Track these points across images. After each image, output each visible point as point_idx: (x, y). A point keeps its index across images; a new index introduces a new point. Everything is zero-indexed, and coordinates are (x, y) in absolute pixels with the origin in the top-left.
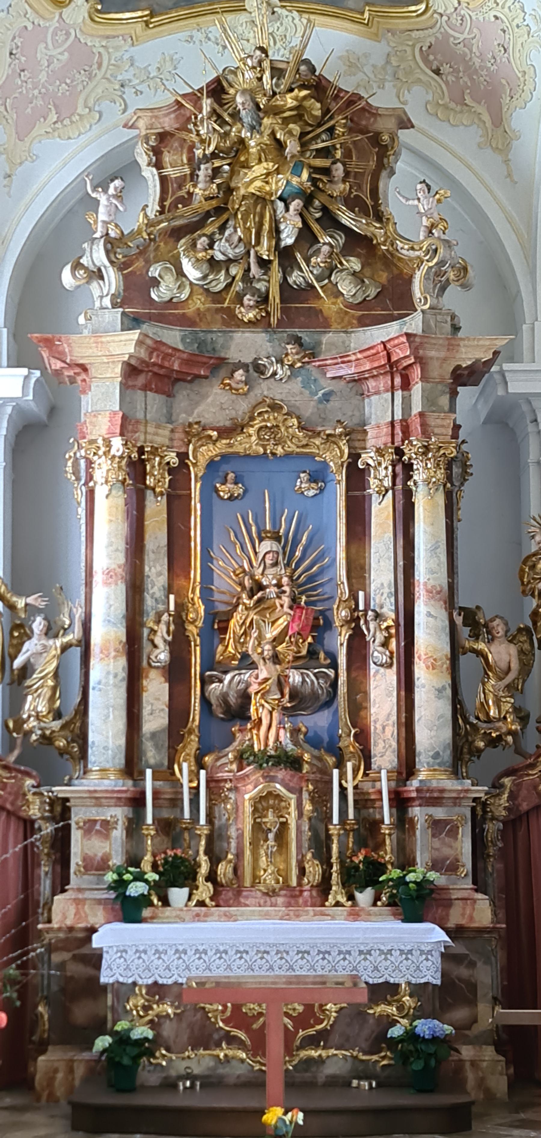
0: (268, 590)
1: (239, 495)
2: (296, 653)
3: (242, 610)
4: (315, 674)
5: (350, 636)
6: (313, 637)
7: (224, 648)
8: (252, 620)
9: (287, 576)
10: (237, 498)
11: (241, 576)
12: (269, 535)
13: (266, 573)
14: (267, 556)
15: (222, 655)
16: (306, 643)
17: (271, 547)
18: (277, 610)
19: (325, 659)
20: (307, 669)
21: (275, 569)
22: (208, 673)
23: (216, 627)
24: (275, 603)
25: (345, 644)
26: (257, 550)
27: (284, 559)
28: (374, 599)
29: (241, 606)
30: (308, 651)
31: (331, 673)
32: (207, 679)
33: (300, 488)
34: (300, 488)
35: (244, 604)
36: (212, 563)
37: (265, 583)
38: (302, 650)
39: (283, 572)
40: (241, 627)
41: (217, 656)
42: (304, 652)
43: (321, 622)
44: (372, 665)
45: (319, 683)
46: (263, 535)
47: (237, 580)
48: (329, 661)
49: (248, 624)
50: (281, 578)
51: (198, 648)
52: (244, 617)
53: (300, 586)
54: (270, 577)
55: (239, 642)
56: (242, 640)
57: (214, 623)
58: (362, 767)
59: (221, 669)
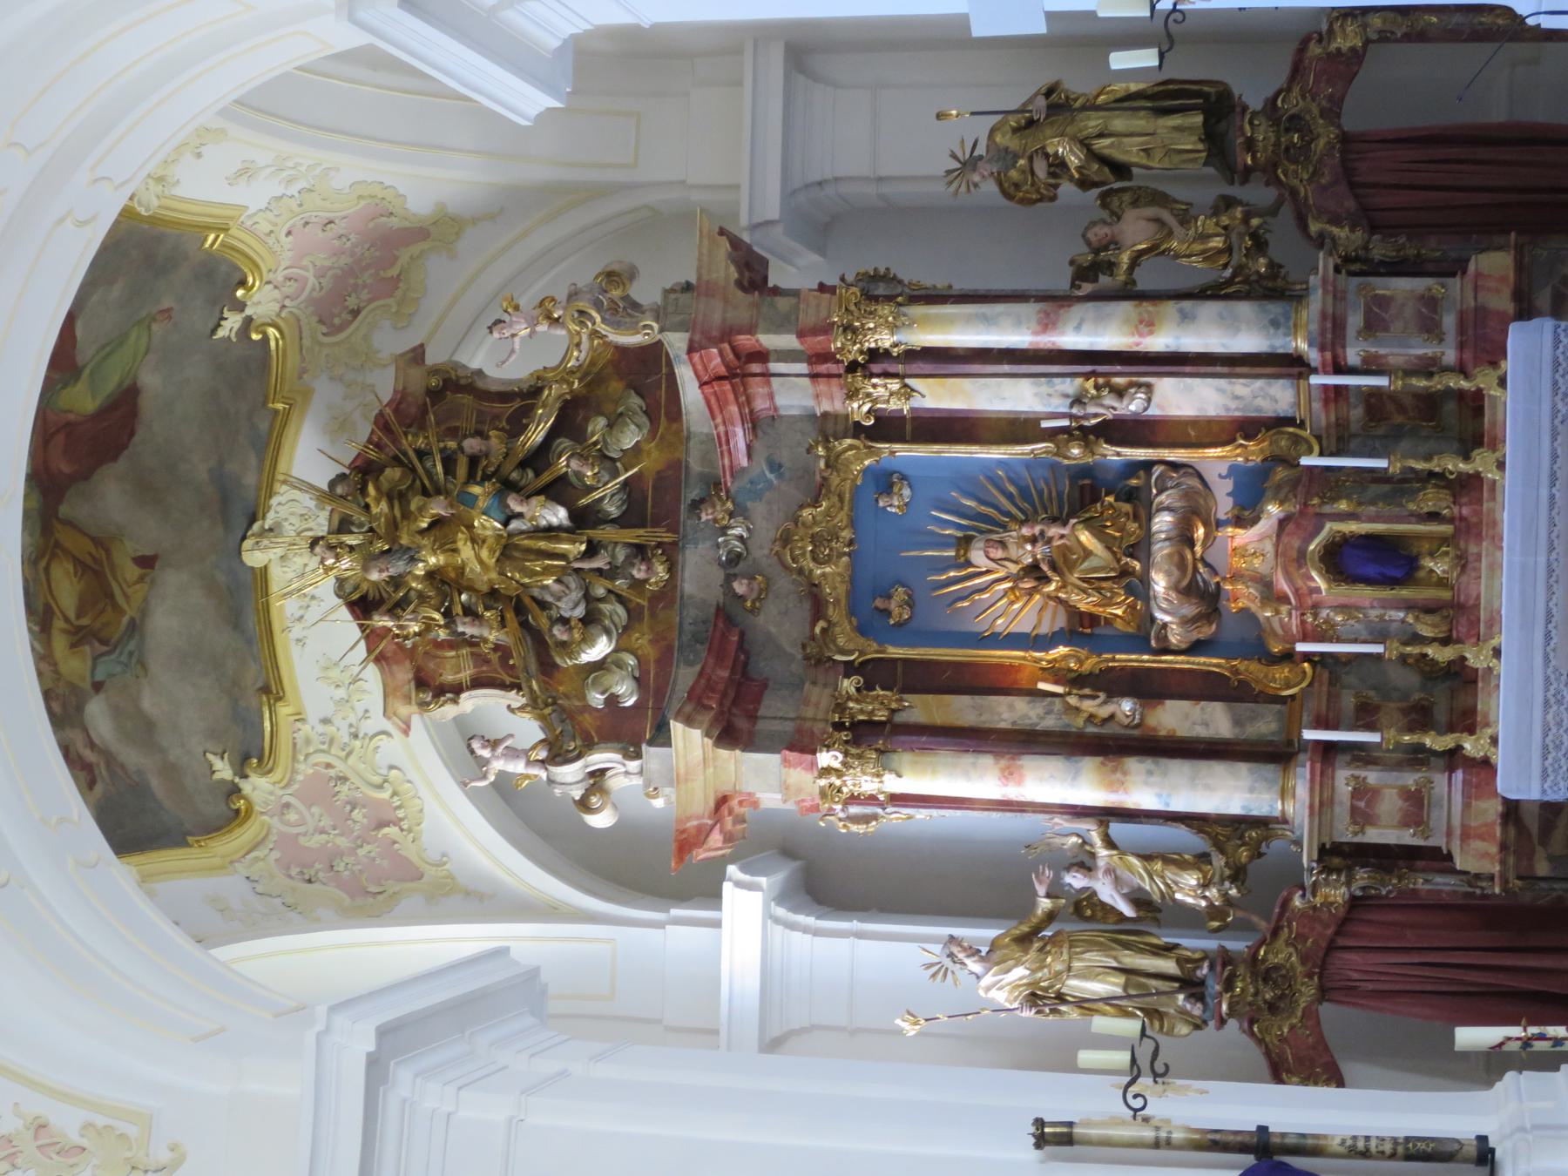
0: (1039, 556)
1: (905, 593)
2: (1128, 519)
3: (1066, 593)
4: (1160, 492)
5: (1106, 442)
6: (1106, 495)
7: (1118, 620)
8: (1080, 579)
9: (1020, 528)
10: (910, 596)
11: (1018, 594)
12: (962, 552)
13: (1014, 558)
14: (992, 555)
15: (1129, 623)
16: (1115, 504)
17: (980, 549)
18: (1068, 543)
19: (1138, 478)
20: (1152, 503)
21: (1010, 546)
22: (1153, 643)
23: (1088, 631)
24: (1058, 547)
25: (1119, 449)
26: (984, 569)
27: (997, 533)
28: (1056, 407)
29: (1060, 595)
30: (1128, 500)
31: (1157, 471)
32: (1162, 645)
33: (898, 507)
34: (898, 507)
35: (1058, 589)
36: (1001, 633)
37: (1030, 560)
38: (1124, 510)
39: (1014, 534)
40: (1089, 595)
41: (1130, 630)
42: (1127, 507)
43: (1087, 482)
44: (1150, 412)
45: (1172, 488)
46: (962, 559)
47: (1025, 599)
48: (1142, 473)
49: (1085, 585)
50: (1024, 537)
51: (1117, 657)
52: (1076, 591)
53: (1036, 512)
54: (1021, 552)
55: (1111, 598)
56: (1109, 594)
57: (1082, 634)
58: (1291, 430)
59: (1148, 624)
